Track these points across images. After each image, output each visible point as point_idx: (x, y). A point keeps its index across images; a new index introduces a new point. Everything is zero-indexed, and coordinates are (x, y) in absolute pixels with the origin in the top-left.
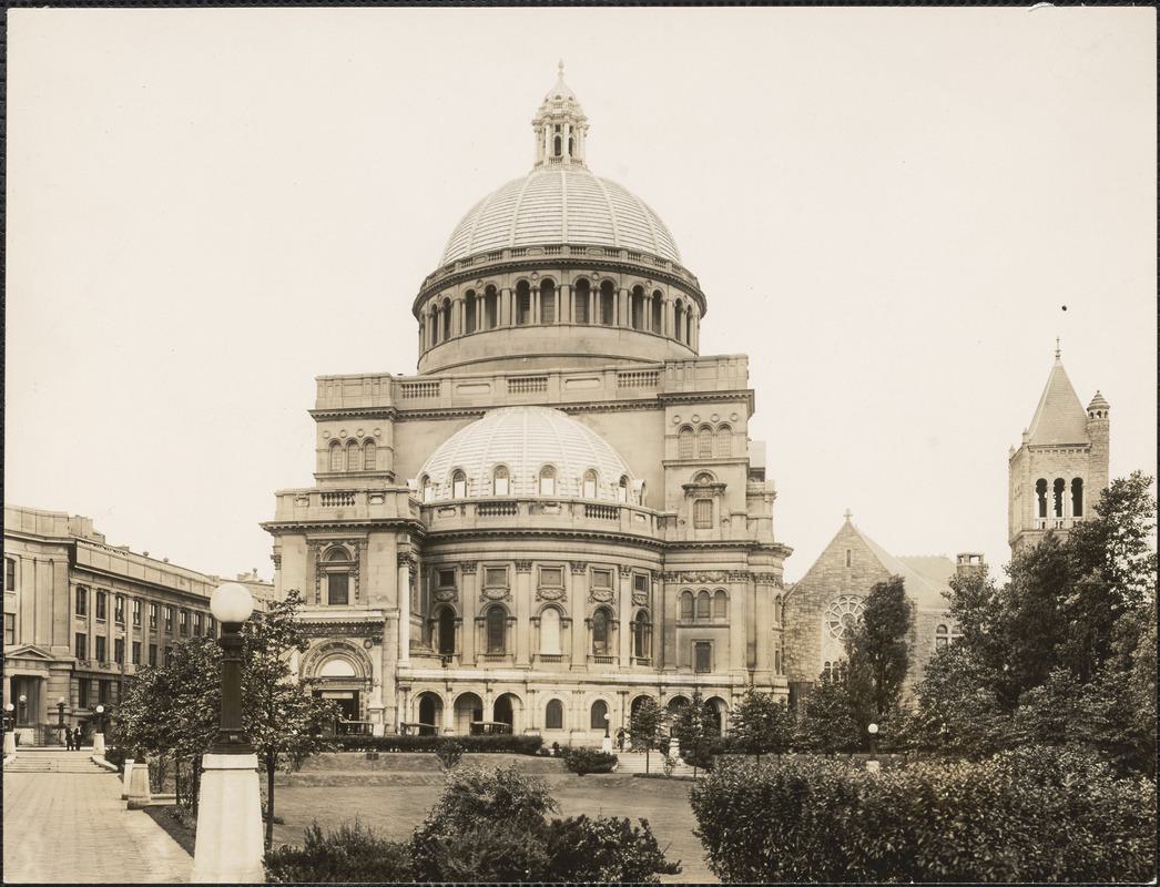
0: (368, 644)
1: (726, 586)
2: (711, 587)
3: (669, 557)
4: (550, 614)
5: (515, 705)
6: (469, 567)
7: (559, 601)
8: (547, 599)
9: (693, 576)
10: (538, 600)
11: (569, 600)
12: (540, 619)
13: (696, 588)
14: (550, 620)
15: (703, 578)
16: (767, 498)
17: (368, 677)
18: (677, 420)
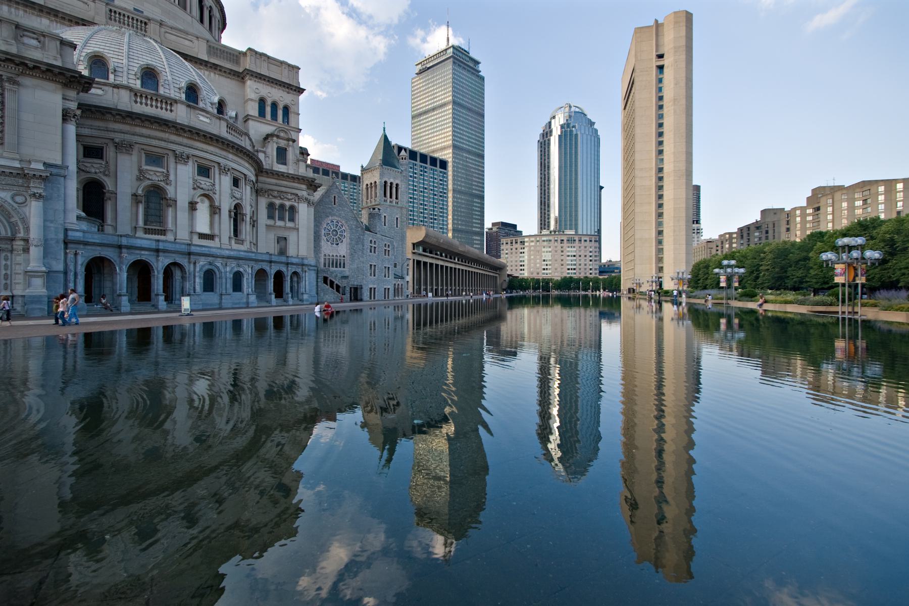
0: (19, 199)
1: (296, 204)
2: (288, 204)
3: (260, 178)
4: (202, 201)
5: (177, 274)
6: (124, 147)
7: (211, 192)
8: (202, 189)
9: (275, 194)
10: (194, 189)
11: (218, 192)
12: (196, 203)
13: (278, 202)
14: (203, 209)
15: (282, 197)
16: (305, 156)
17: (21, 234)
18: (257, 91)
